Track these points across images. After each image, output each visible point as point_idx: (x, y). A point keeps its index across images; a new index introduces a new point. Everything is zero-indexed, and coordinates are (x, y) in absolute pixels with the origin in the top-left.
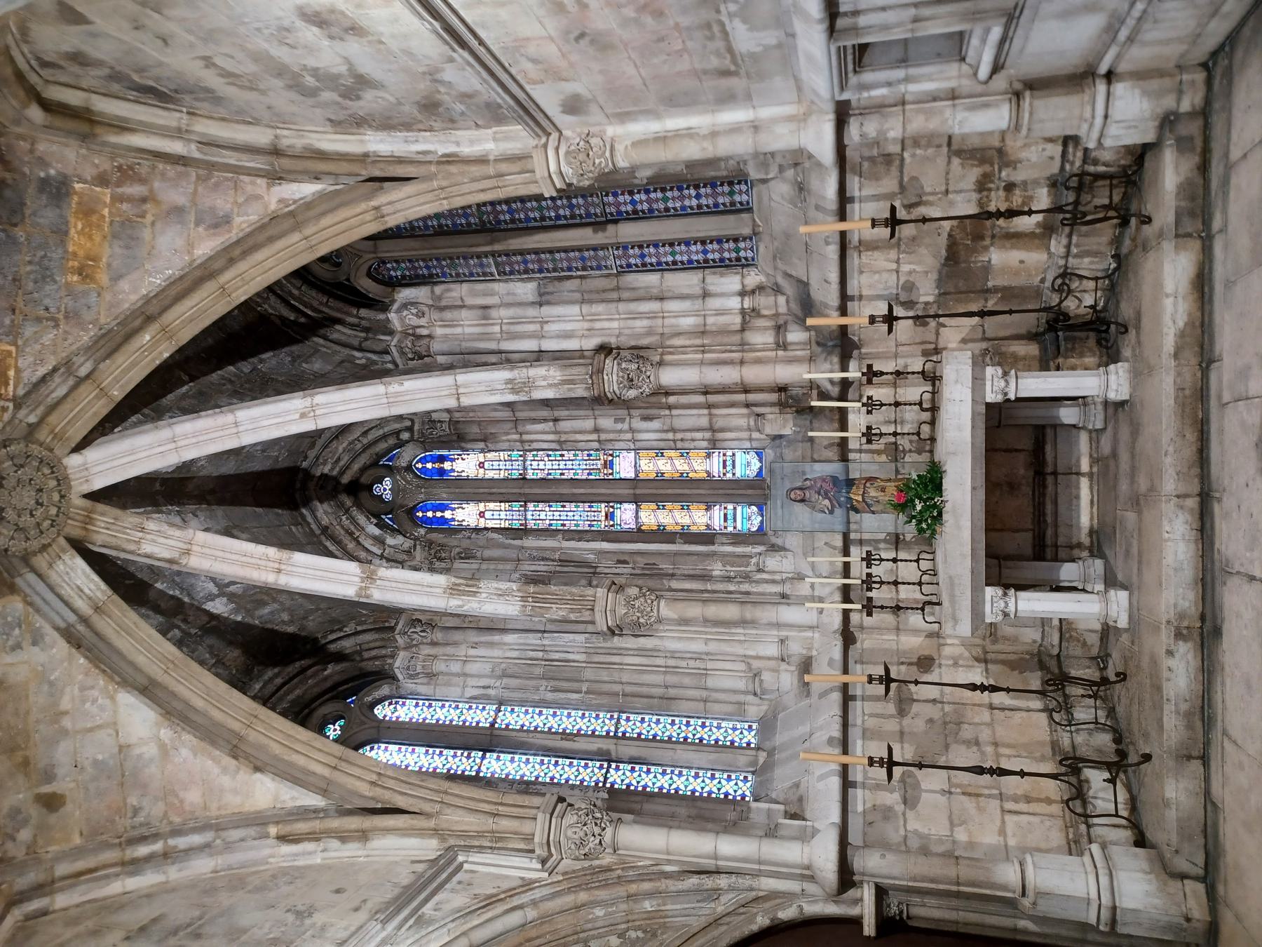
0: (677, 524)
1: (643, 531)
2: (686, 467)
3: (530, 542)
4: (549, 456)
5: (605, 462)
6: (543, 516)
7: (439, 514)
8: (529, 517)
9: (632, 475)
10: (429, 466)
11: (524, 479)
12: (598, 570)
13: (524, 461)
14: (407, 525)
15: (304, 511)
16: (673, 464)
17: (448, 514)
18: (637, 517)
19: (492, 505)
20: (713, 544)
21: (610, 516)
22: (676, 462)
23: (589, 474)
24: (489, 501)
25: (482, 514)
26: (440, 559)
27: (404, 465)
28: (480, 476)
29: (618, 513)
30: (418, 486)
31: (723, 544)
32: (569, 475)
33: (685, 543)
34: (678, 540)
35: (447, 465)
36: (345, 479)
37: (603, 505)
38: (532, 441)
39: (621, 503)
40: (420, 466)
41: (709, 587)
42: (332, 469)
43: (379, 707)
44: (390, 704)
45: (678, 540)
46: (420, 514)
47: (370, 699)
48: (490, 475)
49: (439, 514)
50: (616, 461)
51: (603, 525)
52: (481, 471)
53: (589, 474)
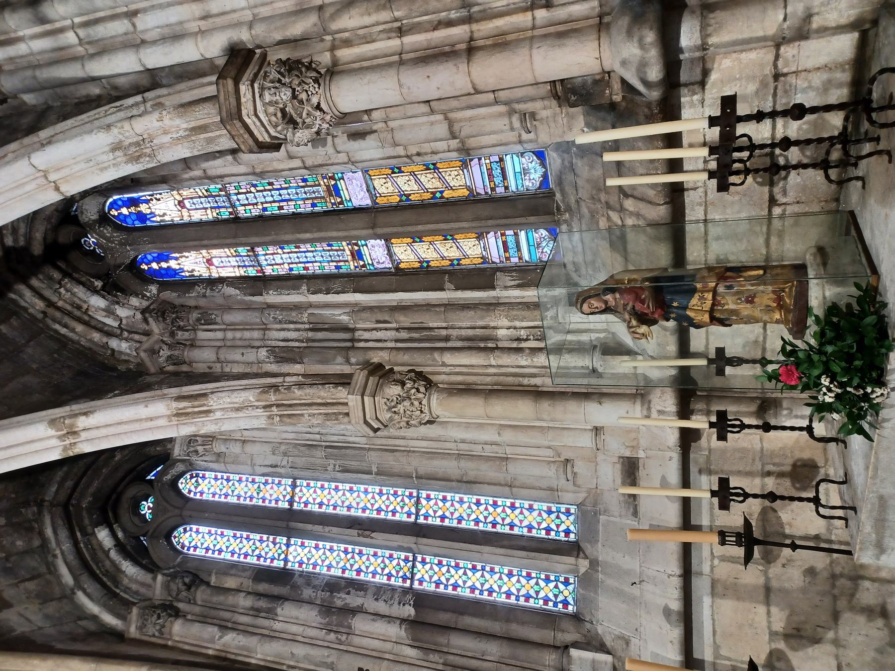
0: (443, 258)
2: (437, 184)
3: (272, 297)
5: (328, 187)
6: (279, 261)
9: (367, 202)
10: (124, 211)
12: (358, 334)
14: (134, 283)
15: (13, 296)
16: (417, 181)
17: (173, 264)
18: (390, 254)
19: (215, 252)
20: (493, 288)
21: (357, 255)
22: (423, 179)
25: (209, 262)
26: (180, 328)
27: (95, 217)
28: (186, 219)
29: (365, 250)
30: (121, 244)
31: (506, 288)
32: (289, 208)
33: (457, 289)
34: (448, 285)
35: (143, 208)
36: (37, 249)
40: (114, 212)
41: (493, 363)
42: (15, 240)
43: (182, 480)
44: (192, 477)
45: (448, 285)
46: (144, 267)
47: (169, 477)
48: (197, 216)
50: (341, 184)
51: (351, 266)
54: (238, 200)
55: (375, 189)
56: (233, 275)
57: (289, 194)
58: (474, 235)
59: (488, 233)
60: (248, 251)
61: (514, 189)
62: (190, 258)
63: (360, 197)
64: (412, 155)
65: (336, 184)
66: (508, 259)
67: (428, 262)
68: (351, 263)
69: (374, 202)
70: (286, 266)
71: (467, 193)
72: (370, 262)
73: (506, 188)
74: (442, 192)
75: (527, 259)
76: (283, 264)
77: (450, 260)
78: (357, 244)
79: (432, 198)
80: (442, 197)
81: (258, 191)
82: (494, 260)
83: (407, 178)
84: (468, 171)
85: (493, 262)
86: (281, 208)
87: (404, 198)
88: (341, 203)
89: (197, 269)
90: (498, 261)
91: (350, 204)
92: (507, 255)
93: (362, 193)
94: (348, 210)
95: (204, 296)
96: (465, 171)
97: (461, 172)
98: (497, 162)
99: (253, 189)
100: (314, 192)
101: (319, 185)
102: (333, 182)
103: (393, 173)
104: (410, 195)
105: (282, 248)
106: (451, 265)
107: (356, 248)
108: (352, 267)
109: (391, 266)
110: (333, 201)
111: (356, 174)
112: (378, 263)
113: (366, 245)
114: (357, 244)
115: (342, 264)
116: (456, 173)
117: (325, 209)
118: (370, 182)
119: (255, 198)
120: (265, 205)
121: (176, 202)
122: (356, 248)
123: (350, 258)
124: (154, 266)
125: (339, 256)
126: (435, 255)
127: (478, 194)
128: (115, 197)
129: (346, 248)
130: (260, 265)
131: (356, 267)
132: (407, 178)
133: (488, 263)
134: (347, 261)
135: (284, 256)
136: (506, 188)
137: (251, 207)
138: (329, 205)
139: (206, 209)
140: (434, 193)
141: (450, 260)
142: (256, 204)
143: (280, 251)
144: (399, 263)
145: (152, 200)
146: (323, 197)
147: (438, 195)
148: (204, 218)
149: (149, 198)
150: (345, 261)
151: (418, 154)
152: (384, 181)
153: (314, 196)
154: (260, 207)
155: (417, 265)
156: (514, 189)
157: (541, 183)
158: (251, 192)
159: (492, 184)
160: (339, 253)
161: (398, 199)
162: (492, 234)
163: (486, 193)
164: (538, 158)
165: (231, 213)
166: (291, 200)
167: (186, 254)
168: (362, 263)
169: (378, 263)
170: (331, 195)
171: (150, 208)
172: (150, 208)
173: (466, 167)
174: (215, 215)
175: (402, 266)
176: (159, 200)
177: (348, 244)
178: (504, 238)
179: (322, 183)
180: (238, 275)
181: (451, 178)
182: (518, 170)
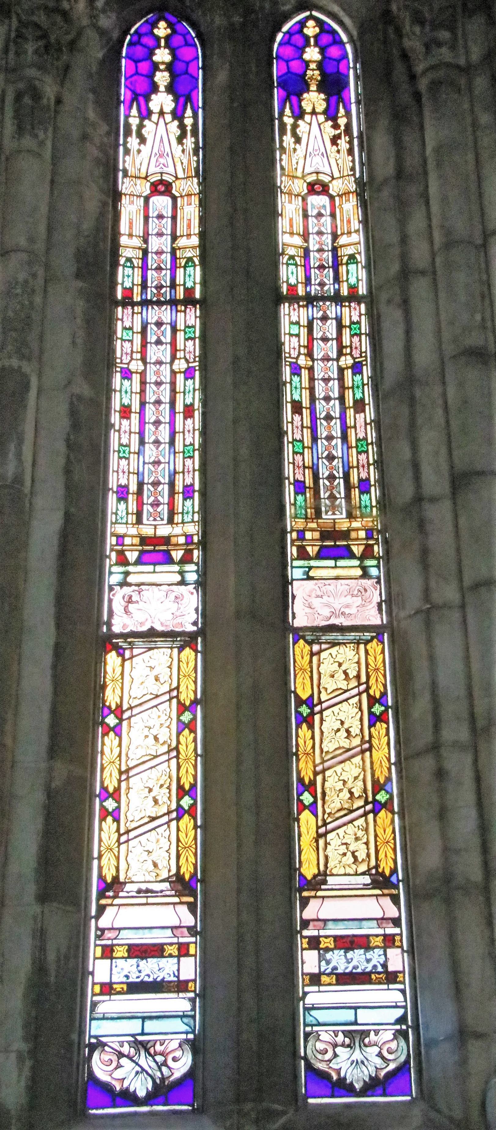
0: (125, 773)
1: (99, 661)
4: (357, 368)
5: (346, 535)
6: (153, 353)
7: (162, 78)
8: (153, 314)
11: (279, 299)
13: (337, 299)
18: (151, 634)
23: (300, 487)
24: (202, 204)
37: (192, 529)
38: (405, 304)
39: (201, 584)
40: (311, 30)
49: (162, 78)
52: (300, 187)
53: (300, 487)
54: (325, 318)
55: (334, 644)
56: (124, 227)
57: (330, 438)
58: (187, 871)
59: (192, 908)
60: (189, 292)
61: (310, 1000)
62: (177, 150)
63: (316, 603)
64: (438, 757)
65: (351, 555)
66: (108, 952)
67: (117, 730)
68: (133, 531)
69: (299, 634)
70: (136, 366)
71: (309, 871)
72: (130, 579)
73: (315, 979)
74: (313, 808)
75: (101, 1009)
76: (144, 360)
77: (117, 790)
78: (187, 559)
79: (301, 780)
80: (302, 807)
81: (341, 370)
82: (109, 912)
83: (355, 730)
84: (366, 887)
85: (101, 910)
86: (297, 408)
87: (305, 710)
88: (303, 554)
89: (146, 149)
90: (104, 922)
91: (298, 573)
92: (120, 952)
93: (326, 612)
94: (284, 566)
95: (85, 137)
96: (367, 880)
97: (363, 868)
98: (385, 966)
99: (347, 361)
100: (332, 497)
101: (350, 516)
102: (357, 550)
103: (372, 701)
104: (311, 726)
105: (189, 374)
106: (104, 789)
107: (177, 555)
108: (121, 529)
109: (117, 629)
110: (308, 535)
111: (374, 611)
112: (130, 601)
113: (183, 582)
114: (187, 559)
115: (132, 506)
116: (361, 855)
117: (289, 511)
118: (352, 636)
119: (326, 359)
120: (305, 373)
121: (326, 179)
122: (177, 555)
123: (147, 531)
124: (162, 55)
125: (156, 504)
126: (135, 756)
127: (305, 902)
128: (349, 48)
129: (178, 530)
130: (145, 303)
131: (120, 538)
132: (355, 730)
133: (101, 895)
134: (139, 521)
135: (165, 371)
136: (315, 979)
137: (304, 341)
138: (300, 524)
139: (305, 236)
140: (311, 787)
141: (117, 790)
142: (310, 354)
143: (180, 365)
144: (121, 654)
145: (336, 126)
146: (318, 514)
147: (307, 798)
148: (283, 224)
149: (342, 121)
150: (139, 515)
151: (440, 774)
152: (352, 673)
153: (324, 494)
154: (302, 361)
155: (111, 698)
156: (310, 1000)
157: (323, 1076)
158: (340, 354)
159: (329, 943)
160: (164, 509)
161: (304, 696)
162: (189, 920)
163: (305, 924)
164: (392, 1075)
165: (292, 288)
166: (315, 439)
167: (189, 142)
168: (132, 556)
169: (130, 601)
170: (325, 535)
171: (314, 113)
172: (314, 113)
173: (375, 884)
174: (291, 251)
175: (112, 659)
176: (334, 141)
177: (189, 538)
178: (173, 950)
179: (356, 524)
180: (124, 240)
181: (348, 840)
182: (364, 1016)
